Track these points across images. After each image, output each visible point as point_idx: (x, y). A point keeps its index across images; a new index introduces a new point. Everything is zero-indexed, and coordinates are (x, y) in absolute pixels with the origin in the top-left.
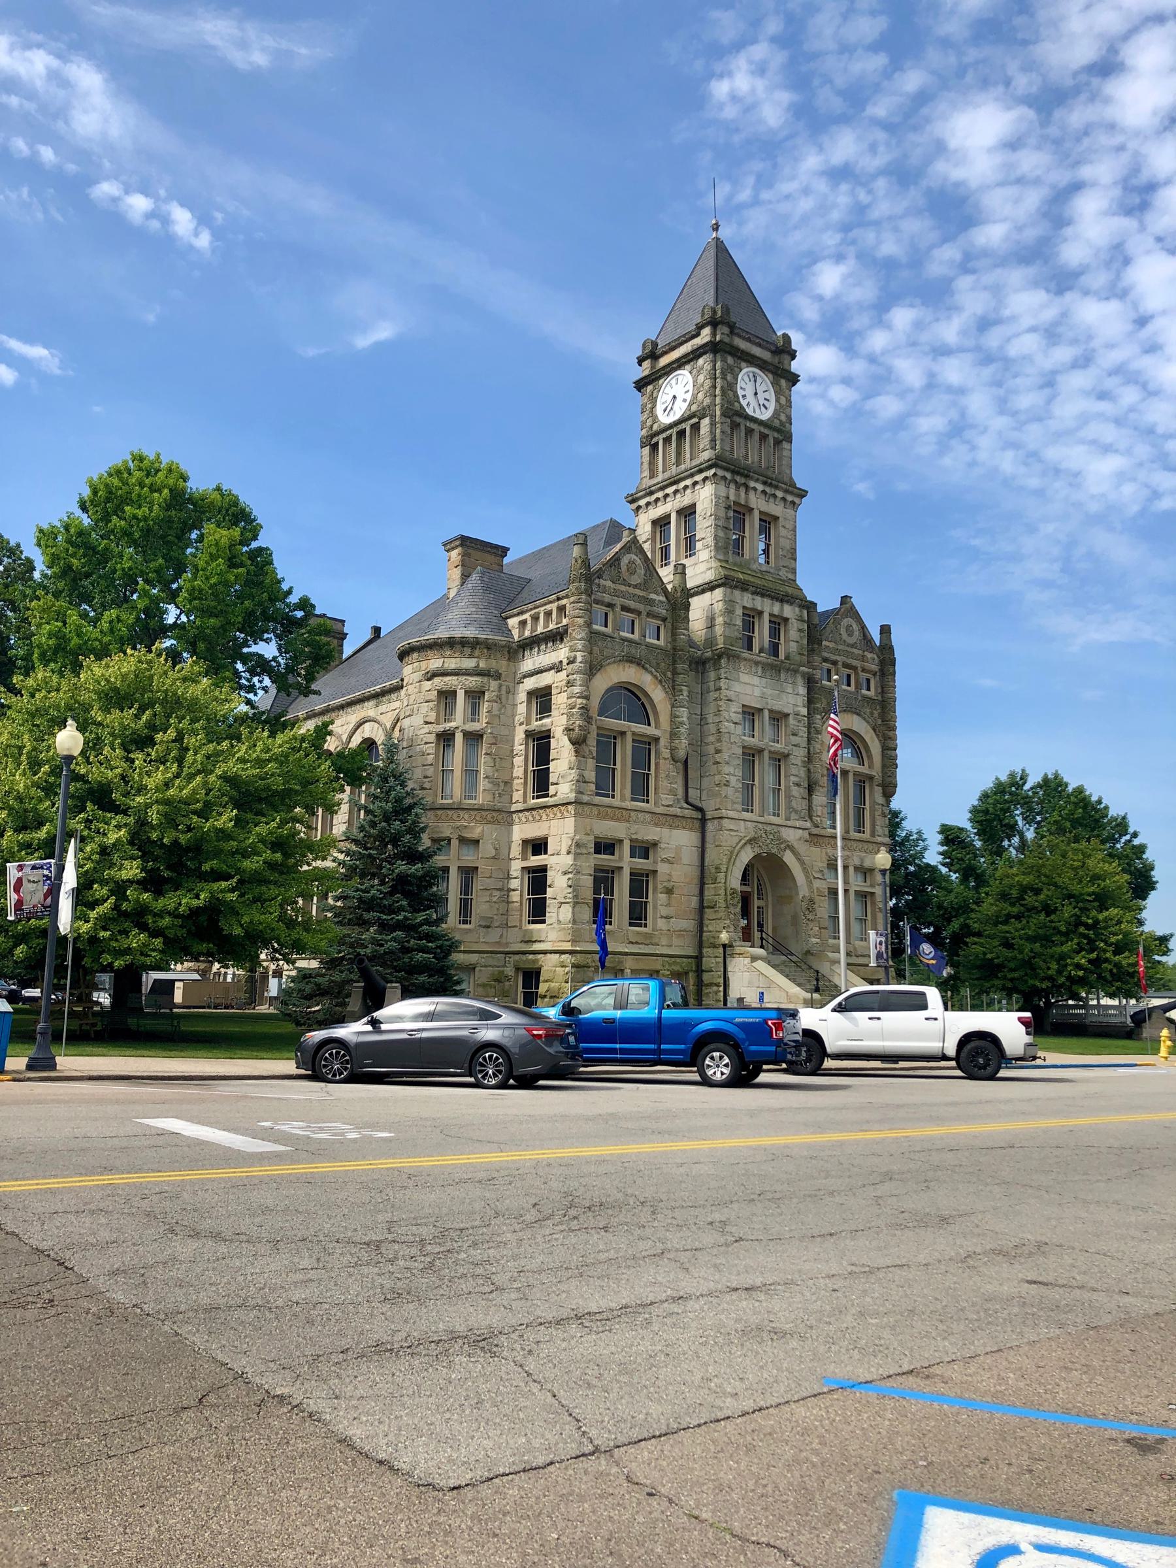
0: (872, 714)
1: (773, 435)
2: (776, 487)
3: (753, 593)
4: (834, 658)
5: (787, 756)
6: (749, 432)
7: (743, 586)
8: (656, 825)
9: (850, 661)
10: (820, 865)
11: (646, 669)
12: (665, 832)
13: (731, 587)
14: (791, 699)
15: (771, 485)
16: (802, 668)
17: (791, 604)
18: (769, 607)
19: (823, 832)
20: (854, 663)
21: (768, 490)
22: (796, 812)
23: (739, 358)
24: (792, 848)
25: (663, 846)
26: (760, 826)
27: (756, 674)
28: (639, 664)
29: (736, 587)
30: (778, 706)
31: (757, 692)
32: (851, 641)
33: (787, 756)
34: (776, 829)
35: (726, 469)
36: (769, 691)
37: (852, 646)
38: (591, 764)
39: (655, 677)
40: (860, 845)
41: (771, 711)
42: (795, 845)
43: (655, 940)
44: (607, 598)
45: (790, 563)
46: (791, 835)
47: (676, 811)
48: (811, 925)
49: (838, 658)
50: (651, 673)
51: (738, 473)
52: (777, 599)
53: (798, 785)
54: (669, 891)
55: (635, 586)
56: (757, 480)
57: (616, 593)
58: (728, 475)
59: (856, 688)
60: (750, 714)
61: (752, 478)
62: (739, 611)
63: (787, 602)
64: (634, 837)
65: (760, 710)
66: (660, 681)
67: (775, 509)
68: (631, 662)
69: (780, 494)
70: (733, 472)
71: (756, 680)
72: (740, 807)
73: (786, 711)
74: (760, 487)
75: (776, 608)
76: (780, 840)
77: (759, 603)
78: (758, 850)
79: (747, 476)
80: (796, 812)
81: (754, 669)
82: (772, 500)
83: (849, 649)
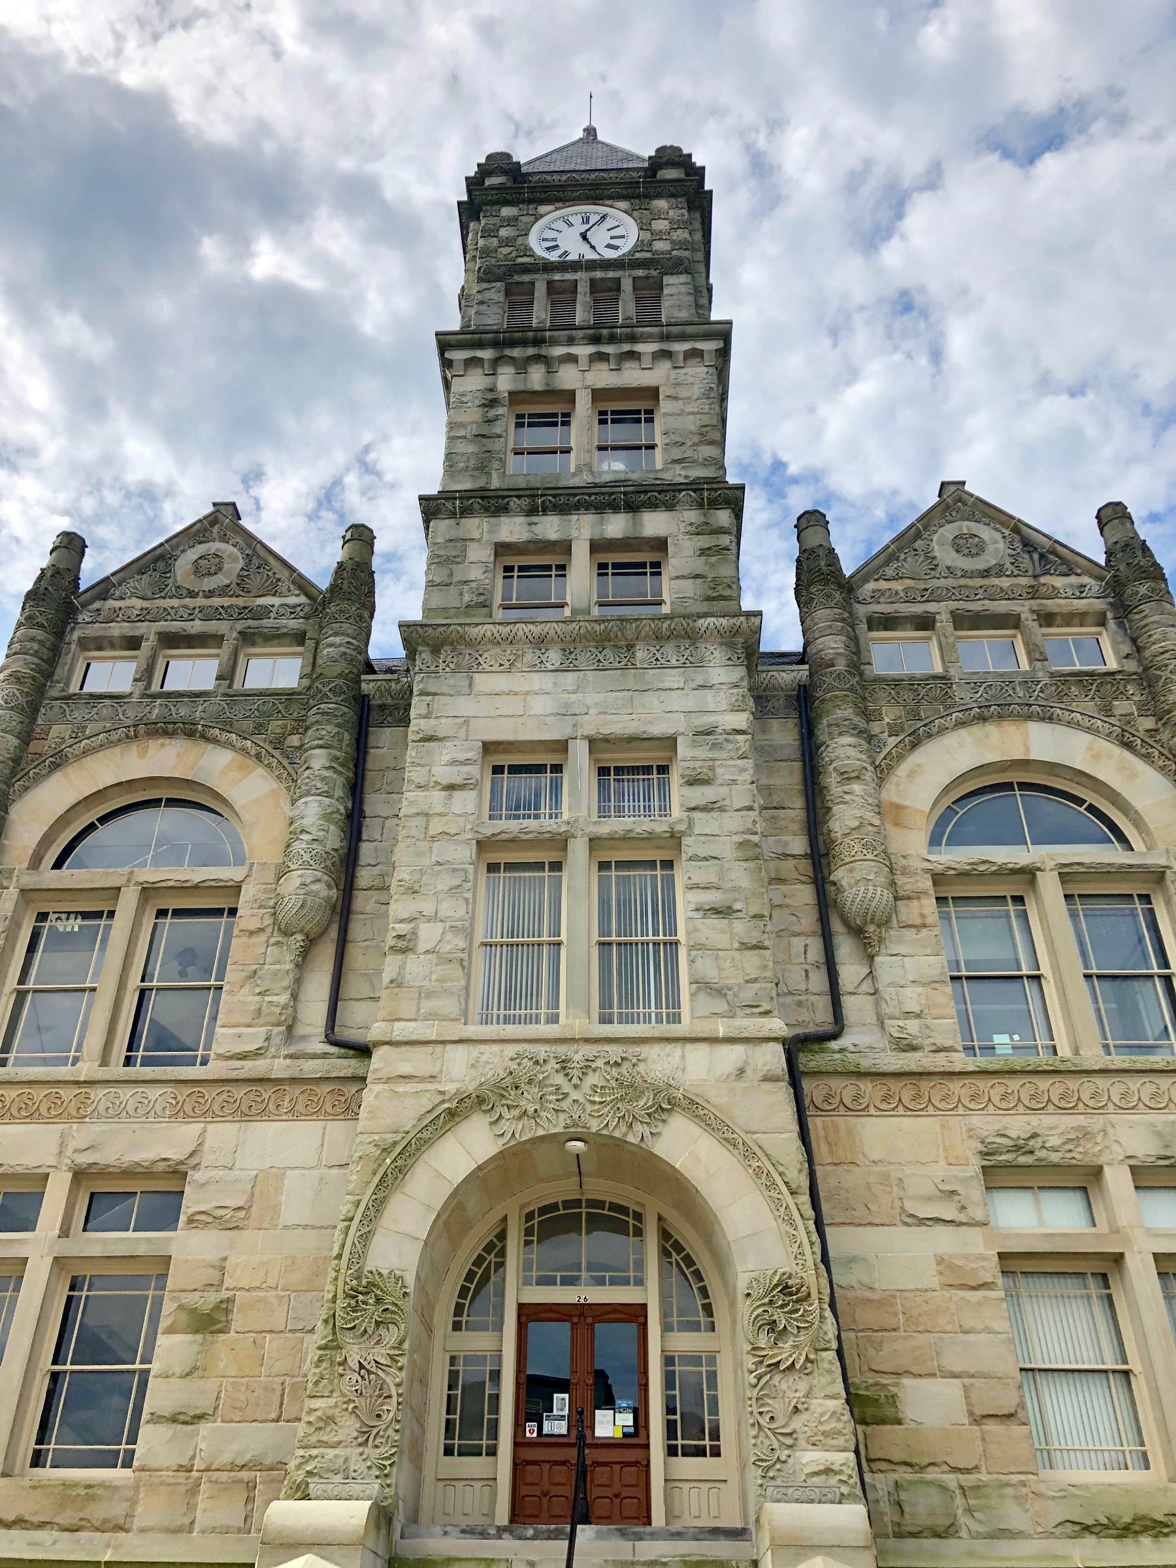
0: (1108, 711)
2: (633, 339)
3: (532, 511)
4: (918, 609)
5: (675, 839)
7: (492, 503)
8: (188, 1118)
10: (941, 1170)
11: (215, 741)
12: (221, 1135)
13: (453, 515)
14: (677, 702)
15: (612, 339)
16: (702, 623)
17: (670, 507)
18: (582, 529)
19: (939, 1062)
20: (1002, 607)
21: (609, 349)
22: (715, 990)
23: (530, 201)
24: (693, 1107)
26: (541, 1051)
27: (538, 667)
28: (190, 734)
29: (466, 512)
30: (621, 724)
31: (540, 706)
32: (979, 564)
33: (675, 839)
35: (480, 345)
36: (592, 698)
37: (986, 573)
39: (244, 751)
41: (595, 743)
42: (717, 1097)
43: (97, 1512)
44: (117, 629)
45: (708, 451)
46: (696, 1069)
47: (279, 1067)
48: (791, 1388)
49: (932, 607)
50: (229, 745)
51: (513, 344)
52: (615, 508)
53: (722, 912)
54: (209, 1322)
55: (210, 594)
56: (571, 341)
57: (145, 616)
58: (487, 354)
59: (1031, 661)
60: (520, 767)
61: (554, 342)
62: (479, 554)
63: (653, 506)
65: (562, 746)
66: (258, 757)
67: (633, 376)
68: (167, 733)
70: (495, 344)
71: (537, 681)
72: (449, 1006)
73: (659, 729)
74: (583, 351)
75: (616, 526)
76: (631, 1089)
77: (550, 527)
78: (527, 1131)
79: (538, 342)
80: (715, 990)
81: (530, 657)
83: (980, 582)
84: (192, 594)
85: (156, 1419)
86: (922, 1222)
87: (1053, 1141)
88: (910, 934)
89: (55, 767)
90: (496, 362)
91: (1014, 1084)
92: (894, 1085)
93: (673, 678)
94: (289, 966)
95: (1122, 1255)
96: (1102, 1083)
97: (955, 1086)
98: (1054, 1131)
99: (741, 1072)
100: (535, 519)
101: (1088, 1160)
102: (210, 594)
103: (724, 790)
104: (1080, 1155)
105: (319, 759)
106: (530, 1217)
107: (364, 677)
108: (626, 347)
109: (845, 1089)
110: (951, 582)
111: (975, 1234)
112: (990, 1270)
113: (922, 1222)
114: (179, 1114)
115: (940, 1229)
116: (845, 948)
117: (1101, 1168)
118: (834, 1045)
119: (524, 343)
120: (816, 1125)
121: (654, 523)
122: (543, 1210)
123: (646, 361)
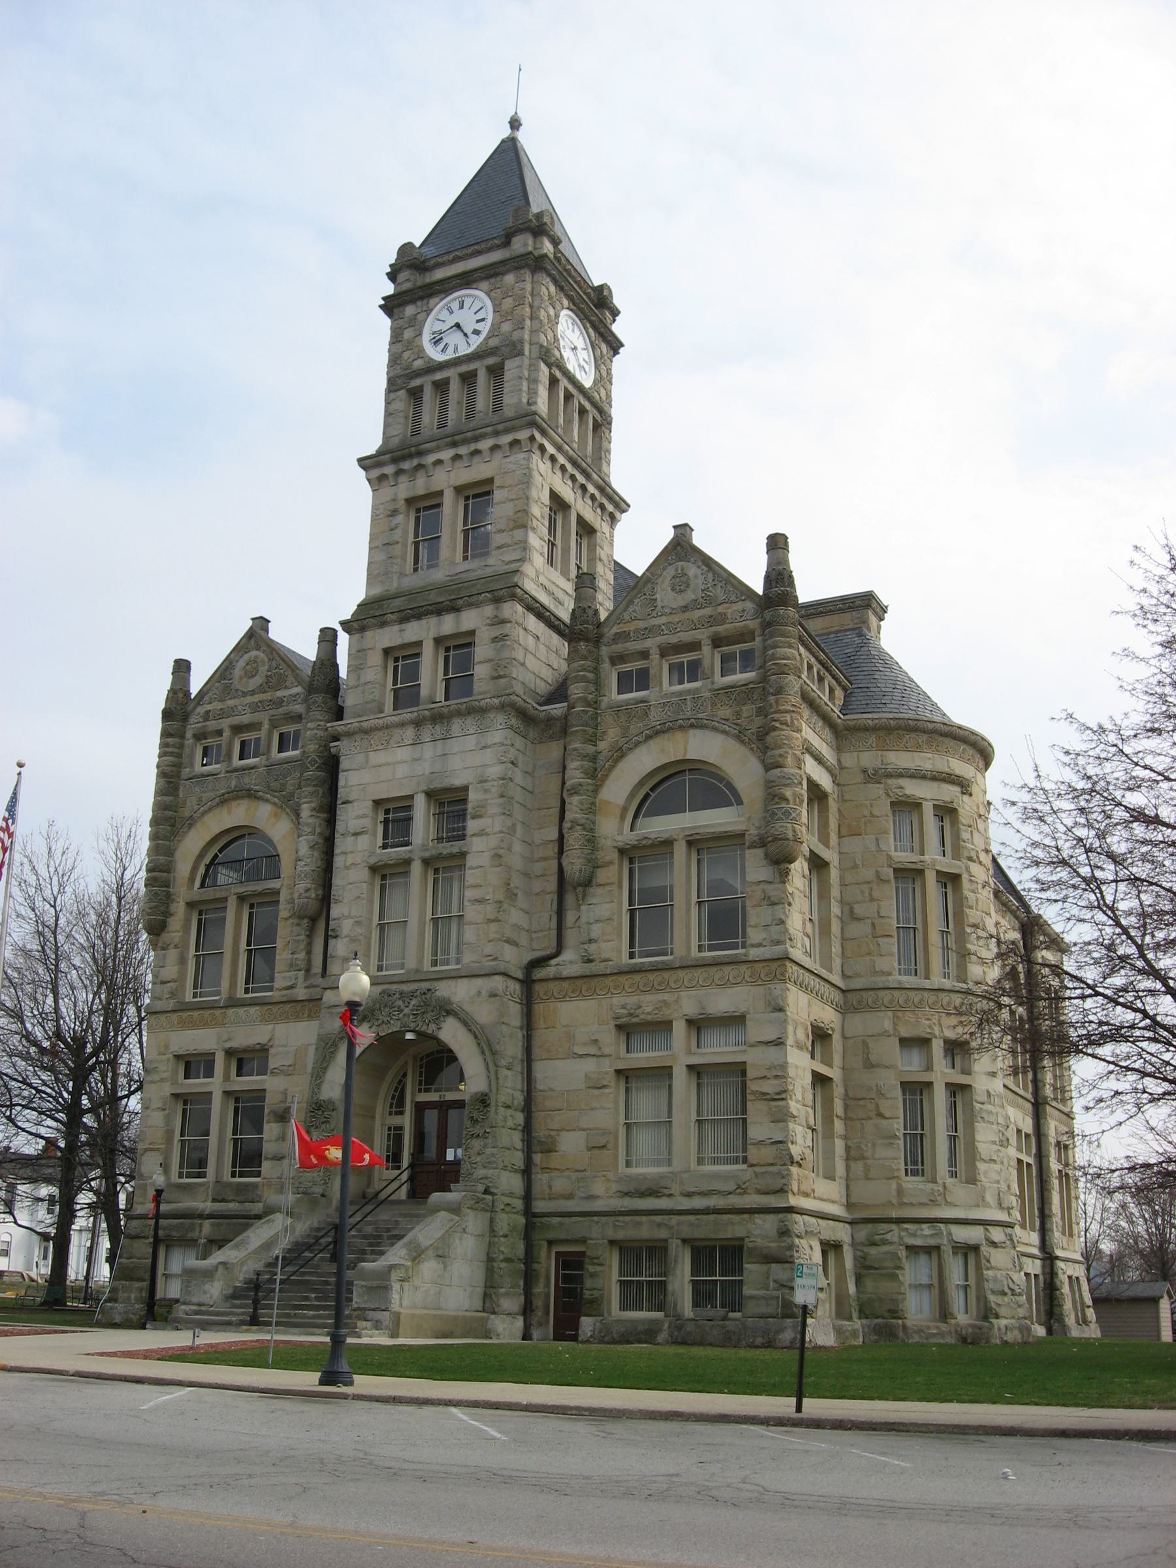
1: (480, 366)
2: (476, 439)
6: (441, 387)
9: (674, 639)
17: (477, 605)
21: (463, 450)
25: (272, 1051)
34: (425, 986)
37: (685, 609)
38: (172, 954)
40: (699, 974)
41: (430, 794)
50: (267, 801)
51: (404, 458)
55: (253, 693)
56: (438, 449)
64: (228, 1045)
67: (478, 471)
69: (485, 445)
70: (395, 461)
71: (403, 754)
74: (446, 455)
82: (476, 459)
84: (244, 694)
85: (267, 1159)
86: (581, 1056)
87: (649, 1009)
88: (599, 891)
89: (190, 826)
90: (399, 472)
91: (637, 978)
92: (579, 982)
93: (471, 742)
94: (303, 937)
95: (671, 1067)
96: (681, 973)
97: (609, 981)
98: (648, 1004)
99: (479, 993)
100: (403, 626)
101: (665, 1018)
102: (253, 693)
103: (489, 820)
104: (658, 1017)
105: (306, 811)
106: (422, 1059)
107: (332, 744)
108: (473, 447)
109: (554, 987)
110: (663, 620)
111: (607, 1061)
112: (610, 1079)
113: (581, 1056)
114: (264, 1020)
115: (590, 1060)
116: (570, 899)
117: (671, 1022)
118: (553, 962)
119: (410, 456)
120: (539, 1008)
121: (469, 619)
122: (428, 1055)
123: (486, 454)
